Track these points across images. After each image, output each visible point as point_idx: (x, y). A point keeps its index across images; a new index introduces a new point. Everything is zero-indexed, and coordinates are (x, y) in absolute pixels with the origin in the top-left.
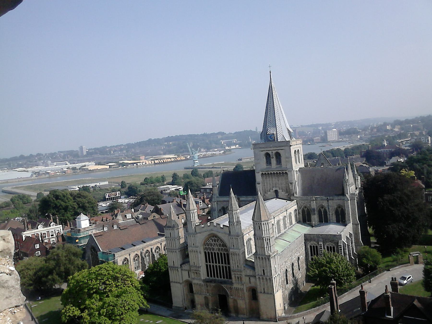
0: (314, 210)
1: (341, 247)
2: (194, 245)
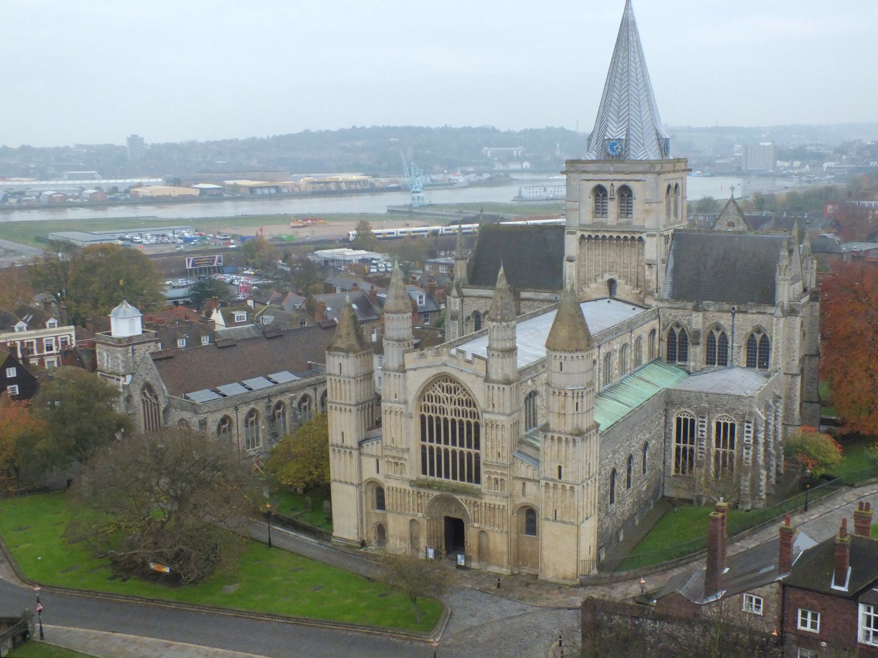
0: (697, 333)
1: (750, 425)
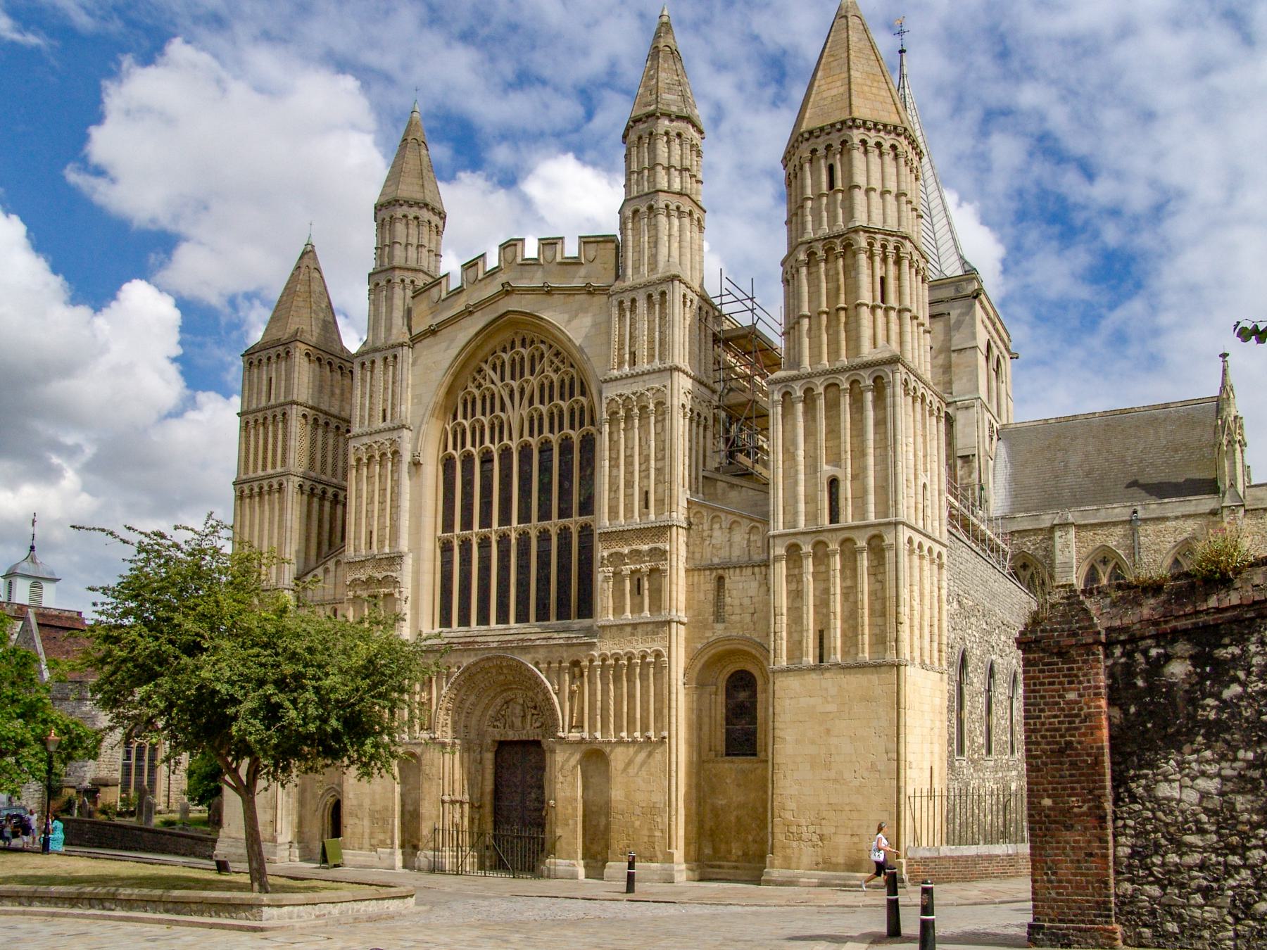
2: (384, 420)
